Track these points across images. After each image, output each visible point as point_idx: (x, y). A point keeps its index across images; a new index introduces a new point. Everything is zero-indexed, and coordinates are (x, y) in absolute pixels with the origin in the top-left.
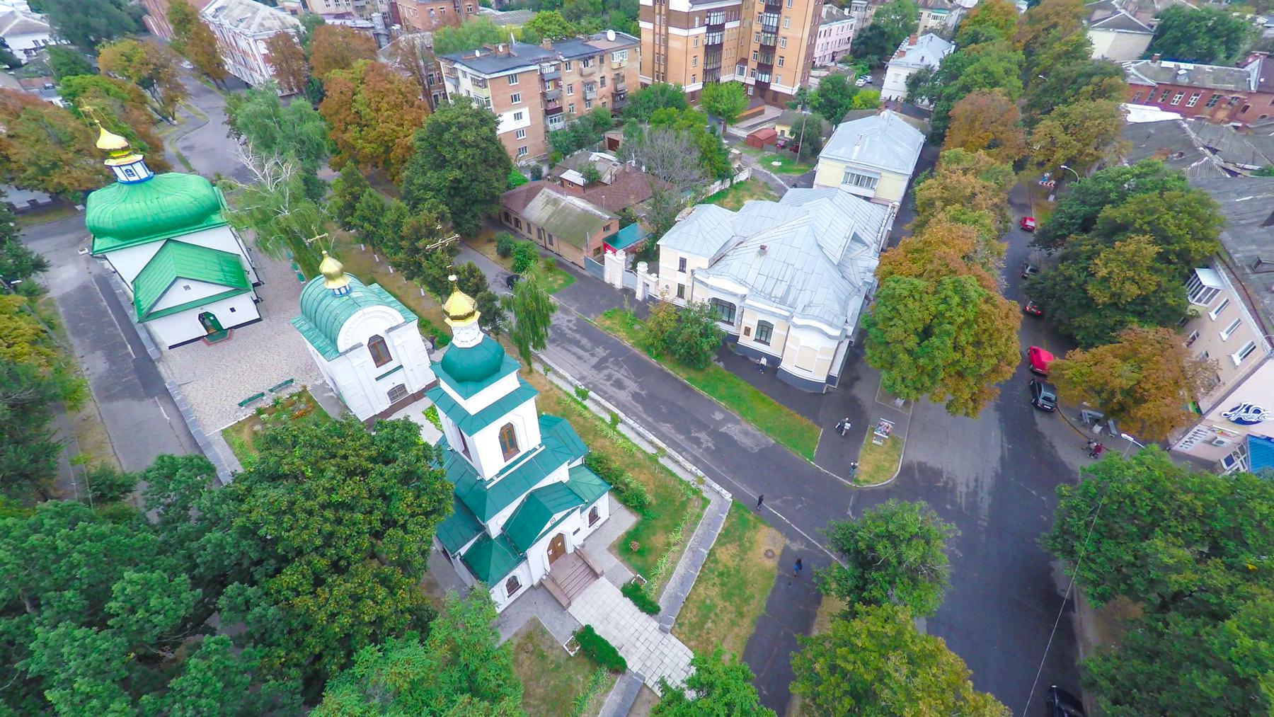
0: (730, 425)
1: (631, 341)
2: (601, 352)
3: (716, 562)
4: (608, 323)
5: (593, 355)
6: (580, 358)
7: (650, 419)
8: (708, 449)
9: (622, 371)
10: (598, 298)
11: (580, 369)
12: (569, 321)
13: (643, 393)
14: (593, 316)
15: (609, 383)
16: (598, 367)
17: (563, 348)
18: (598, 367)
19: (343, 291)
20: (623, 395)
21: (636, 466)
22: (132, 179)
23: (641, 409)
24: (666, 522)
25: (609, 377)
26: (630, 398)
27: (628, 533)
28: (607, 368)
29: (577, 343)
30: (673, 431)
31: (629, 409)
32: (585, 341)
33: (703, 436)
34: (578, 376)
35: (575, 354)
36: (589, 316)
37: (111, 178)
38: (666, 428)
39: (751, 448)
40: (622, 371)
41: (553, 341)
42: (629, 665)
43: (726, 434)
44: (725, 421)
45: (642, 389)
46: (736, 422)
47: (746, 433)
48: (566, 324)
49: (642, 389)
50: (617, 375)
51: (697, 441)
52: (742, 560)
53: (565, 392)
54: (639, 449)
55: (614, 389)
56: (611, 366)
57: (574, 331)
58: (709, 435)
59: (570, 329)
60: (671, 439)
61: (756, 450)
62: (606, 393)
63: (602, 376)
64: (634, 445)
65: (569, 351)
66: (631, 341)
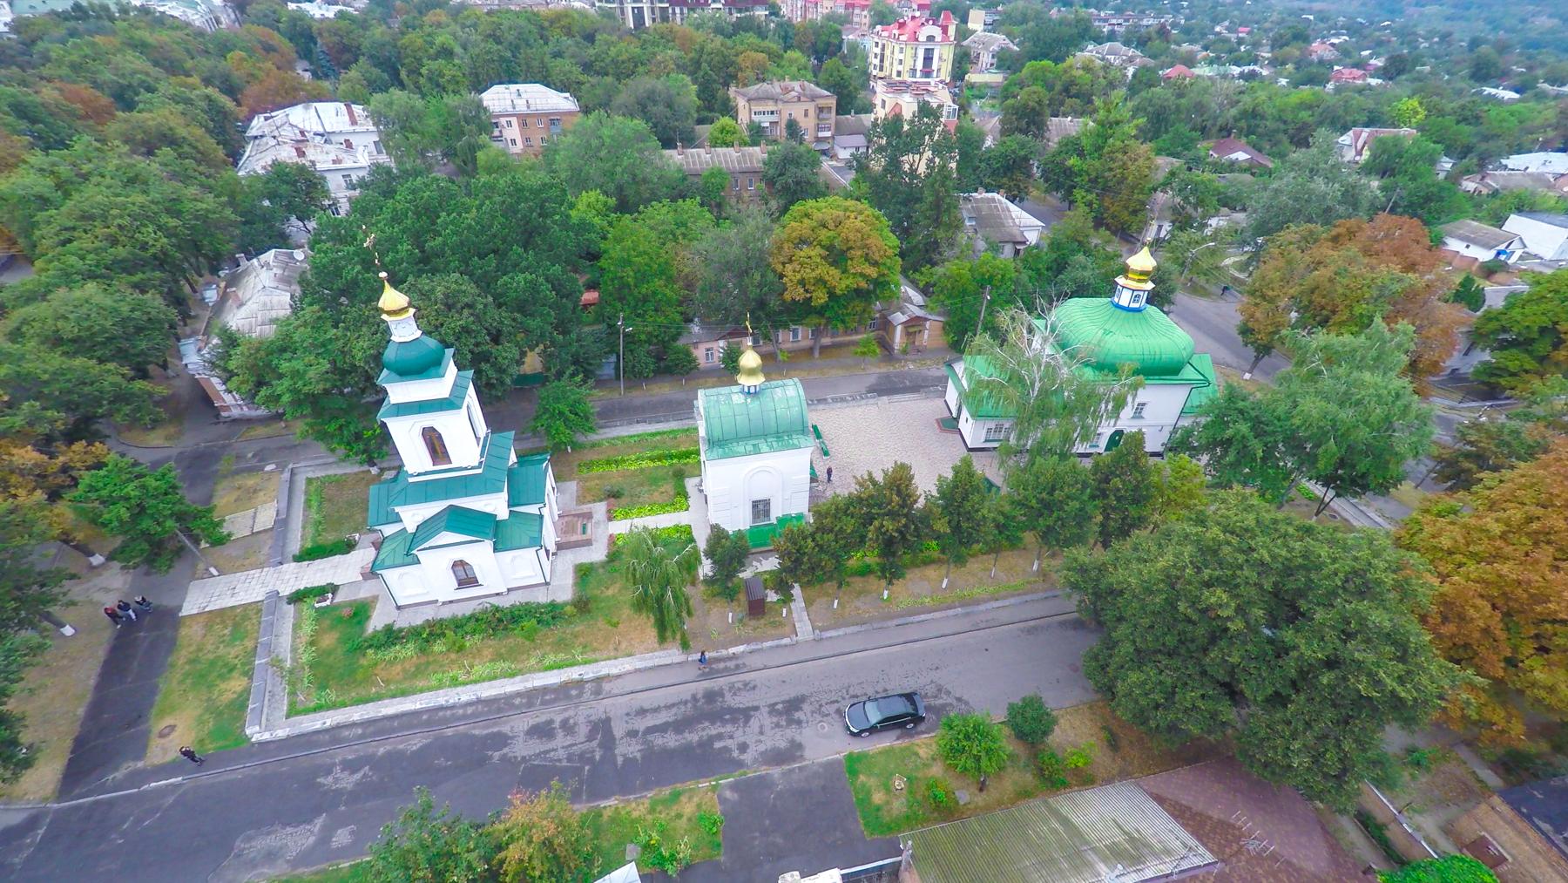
0: (312, 840)
1: (607, 814)
2: (628, 749)
3: (245, 674)
4: (688, 809)
5: (632, 734)
6: (642, 712)
7: (449, 732)
8: (329, 772)
9: (562, 754)
10: (779, 840)
11: (620, 700)
12: (743, 748)
13: (497, 755)
14: (728, 794)
15: (558, 719)
16: (601, 728)
17: (686, 703)
18: (601, 728)
19: (752, 390)
20: (519, 724)
21: (419, 671)
22: (1116, 300)
23: (477, 732)
24: (332, 658)
25: (567, 727)
26: (506, 729)
27: (368, 618)
28: (590, 738)
29: (679, 726)
30: (401, 747)
31: (489, 712)
32: (671, 740)
33: (348, 781)
34: (606, 687)
35: (656, 710)
36: (734, 787)
37: (1104, 287)
38: (415, 743)
39: (249, 839)
40: (562, 754)
41: (711, 696)
42: (294, 564)
43: (309, 821)
44: (324, 839)
45: (504, 758)
46: (304, 858)
47: (271, 856)
48: (740, 737)
49: (504, 758)
50: (561, 740)
51: (351, 767)
52: (209, 699)
53: (596, 661)
54: (429, 689)
55: (543, 718)
56: (586, 746)
57: (712, 739)
58: (339, 793)
59: (720, 737)
60: (394, 730)
61: (239, 843)
62: (544, 703)
63: (581, 720)
64: (439, 687)
65: (669, 707)
66: (607, 814)
